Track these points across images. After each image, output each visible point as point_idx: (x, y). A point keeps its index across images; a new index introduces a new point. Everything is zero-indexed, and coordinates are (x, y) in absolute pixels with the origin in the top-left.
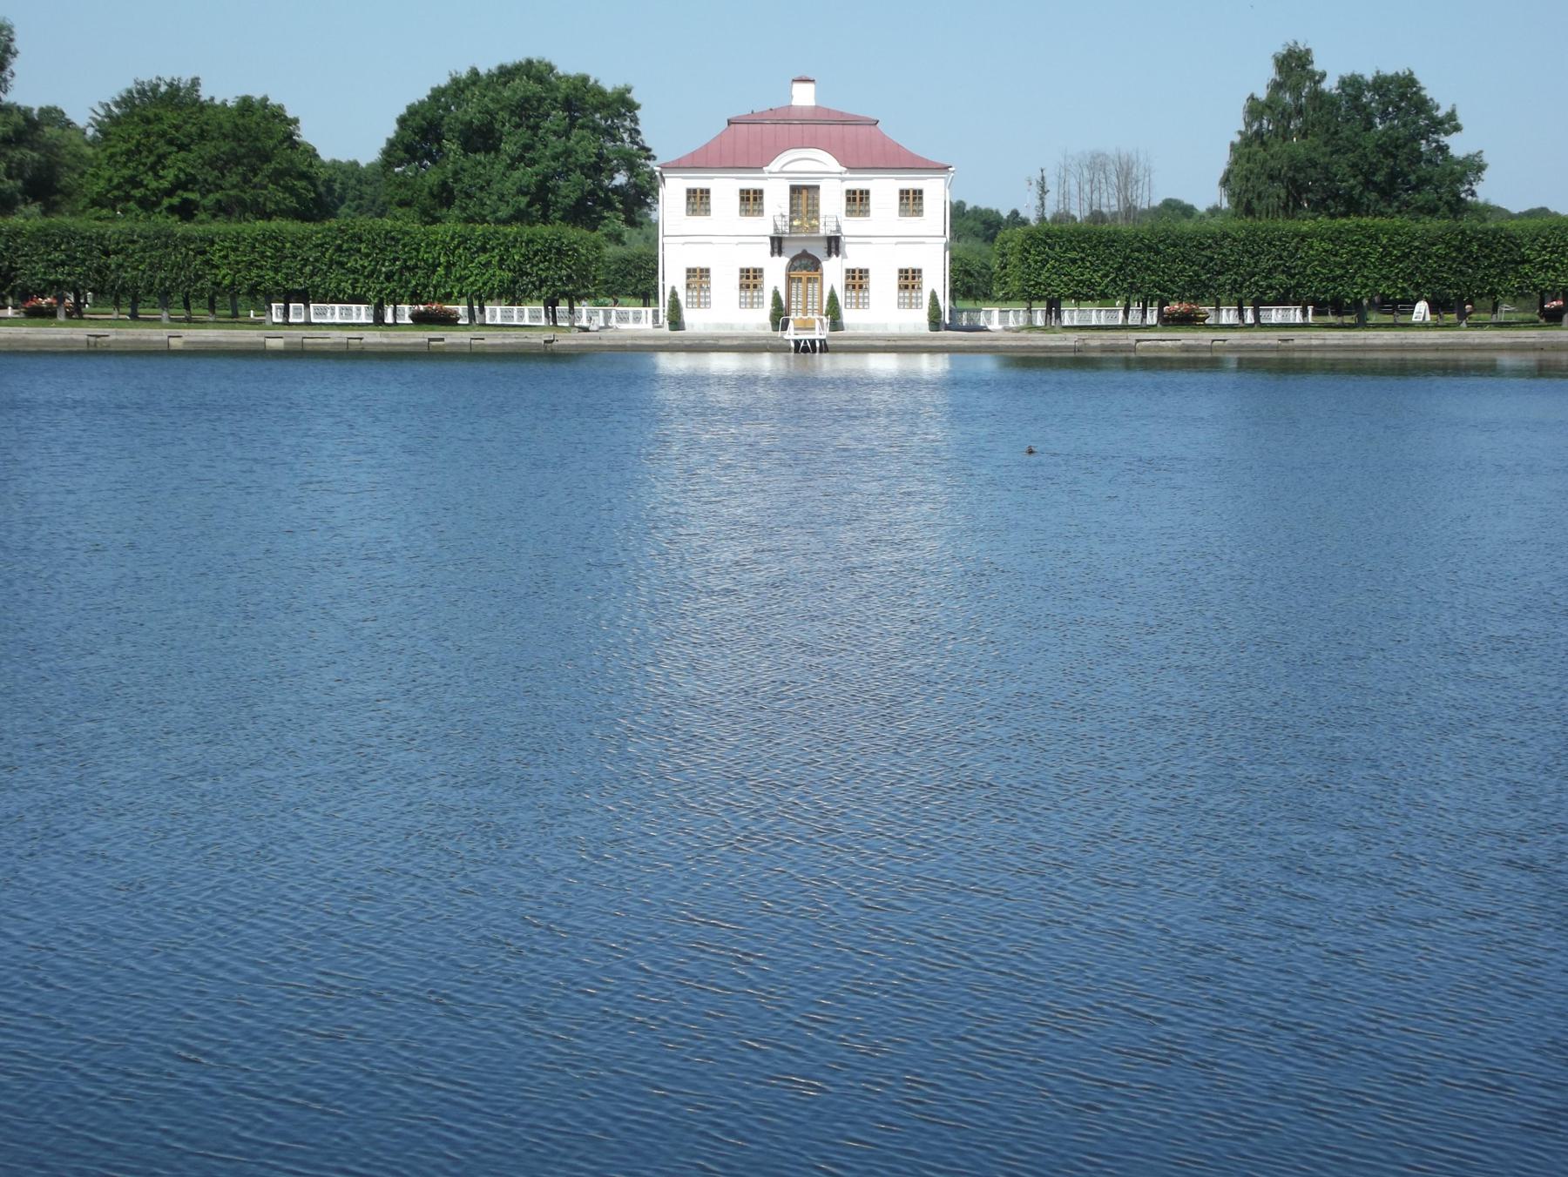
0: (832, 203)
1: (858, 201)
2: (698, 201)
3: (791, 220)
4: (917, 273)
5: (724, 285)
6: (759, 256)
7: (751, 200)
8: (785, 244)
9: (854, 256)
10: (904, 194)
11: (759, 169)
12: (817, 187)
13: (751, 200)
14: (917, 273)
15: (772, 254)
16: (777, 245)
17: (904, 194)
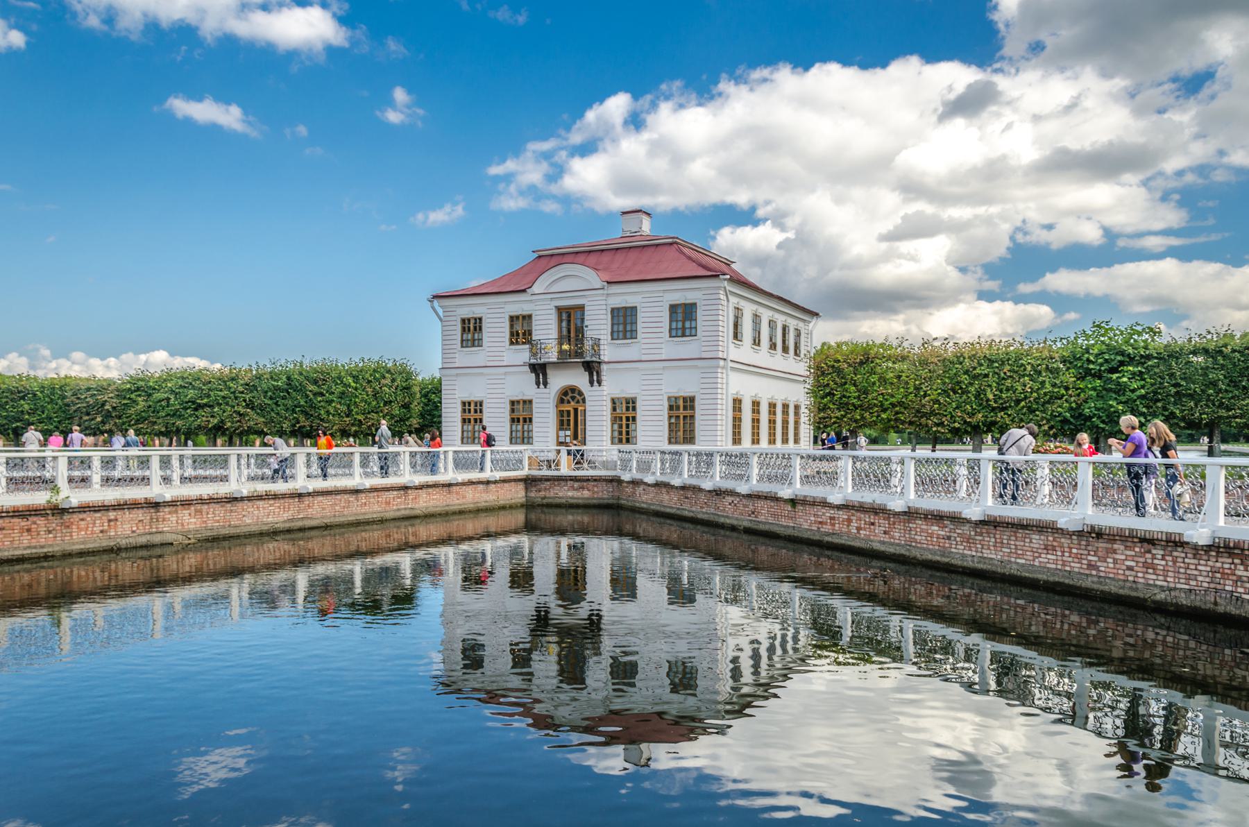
0: (598, 325)
1: (624, 322)
2: (472, 330)
3: (561, 344)
4: (689, 402)
5: (497, 421)
6: (524, 386)
7: (520, 331)
8: (549, 372)
9: (614, 385)
10: (673, 308)
11: (524, 291)
12: (581, 308)
13: (520, 331)
14: (689, 402)
15: (538, 384)
16: (539, 370)
17: (673, 308)
